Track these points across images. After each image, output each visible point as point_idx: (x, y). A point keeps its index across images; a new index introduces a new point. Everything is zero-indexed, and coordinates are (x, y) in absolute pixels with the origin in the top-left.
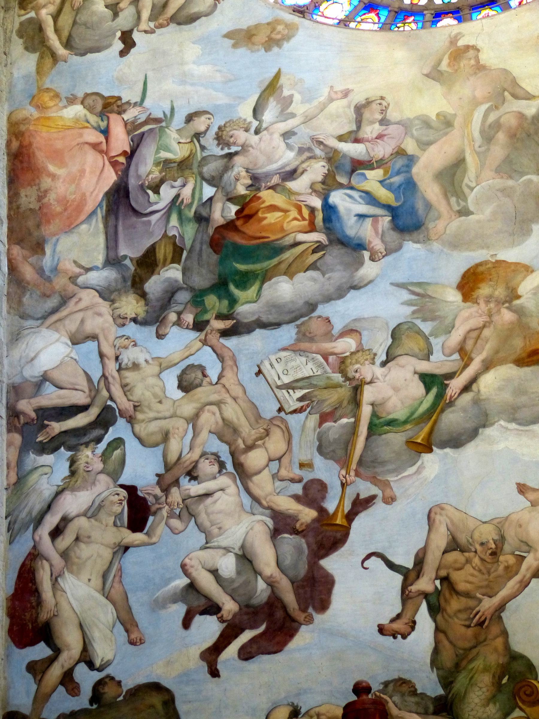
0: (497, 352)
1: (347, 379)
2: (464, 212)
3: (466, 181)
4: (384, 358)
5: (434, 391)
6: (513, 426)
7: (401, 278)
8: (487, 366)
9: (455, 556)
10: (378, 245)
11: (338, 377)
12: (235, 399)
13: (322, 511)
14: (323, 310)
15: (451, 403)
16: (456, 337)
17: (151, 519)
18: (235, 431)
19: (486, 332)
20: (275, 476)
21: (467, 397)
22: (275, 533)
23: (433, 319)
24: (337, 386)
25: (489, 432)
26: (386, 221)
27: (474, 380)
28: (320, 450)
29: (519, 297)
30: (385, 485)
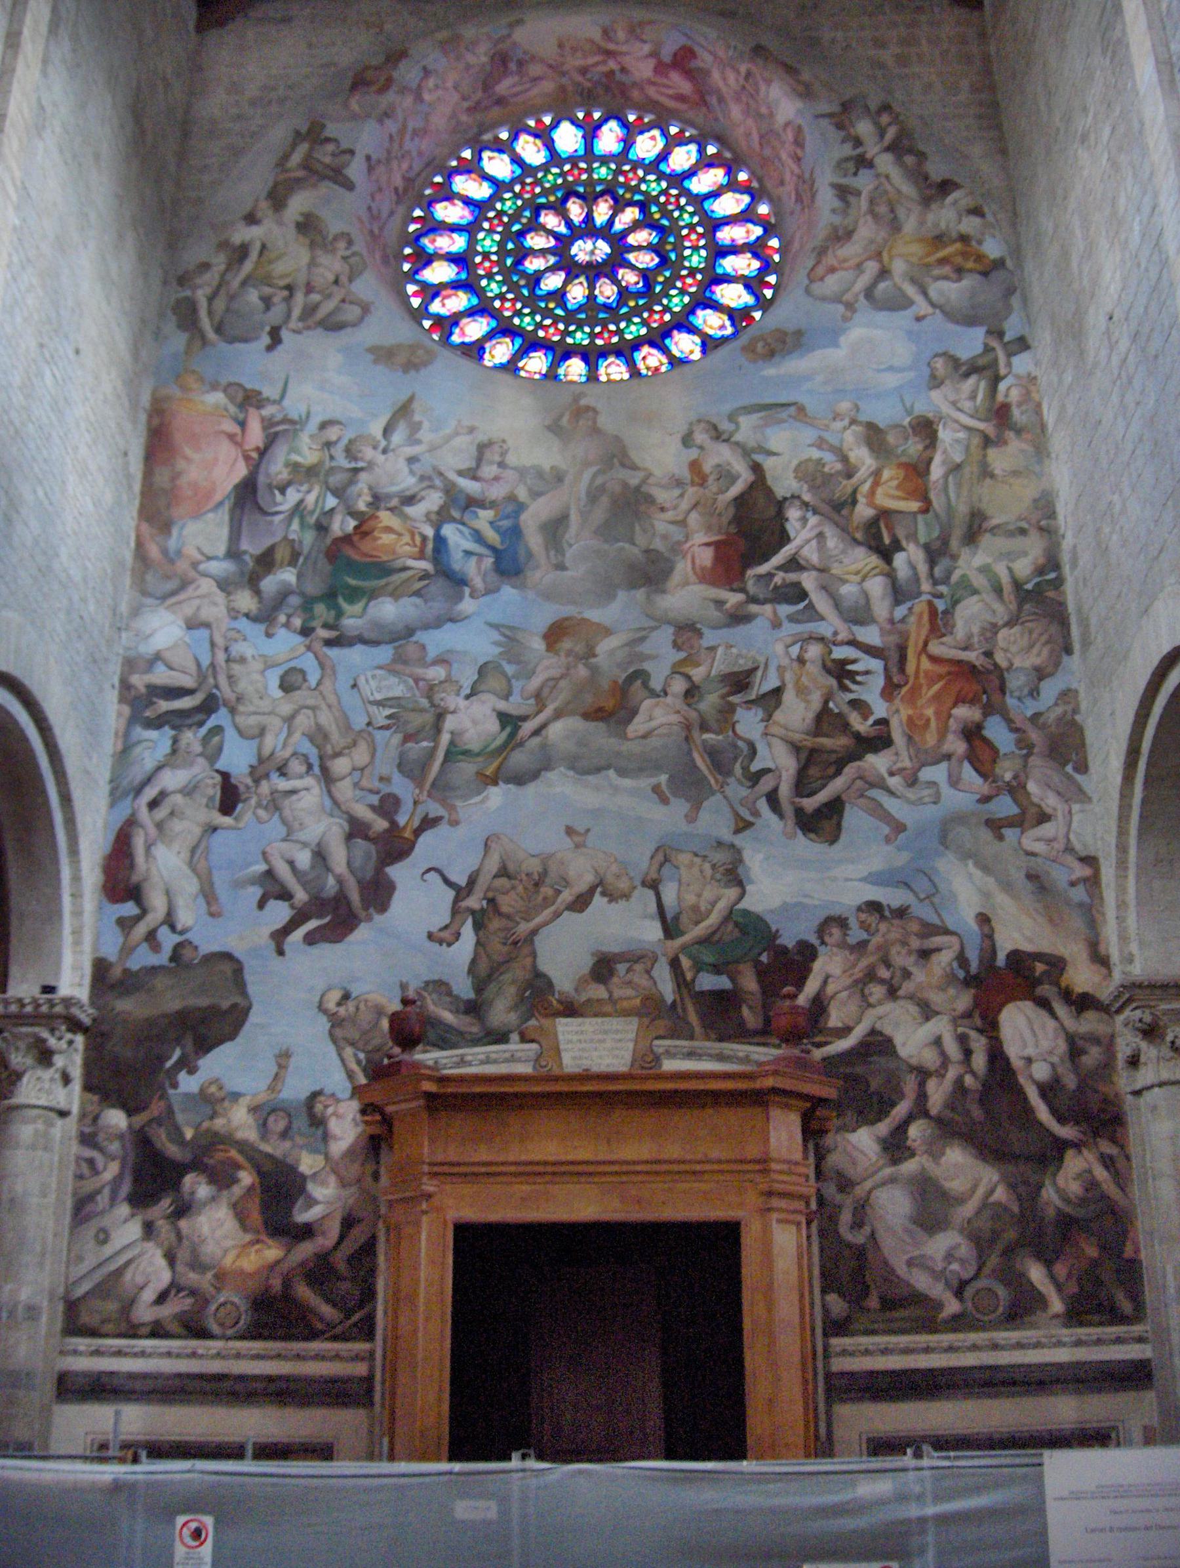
0: (569, 703)
1: (433, 705)
2: (561, 567)
3: (567, 536)
4: (468, 691)
5: (508, 730)
6: (571, 773)
7: (494, 618)
8: (558, 715)
9: (503, 882)
10: (478, 582)
11: (424, 702)
12: (329, 706)
13: (393, 823)
14: (421, 636)
15: (521, 744)
16: (535, 683)
17: (240, 806)
18: (326, 737)
19: (563, 684)
20: (356, 785)
21: (536, 741)
22: (349, 837)
23: (518, 663)
24: (422, 710)
25: (551, 775)
26: (489, 561)
27: (544, 726)
28: (400, 766)
29: (595, 656)
30: (452, 808)
